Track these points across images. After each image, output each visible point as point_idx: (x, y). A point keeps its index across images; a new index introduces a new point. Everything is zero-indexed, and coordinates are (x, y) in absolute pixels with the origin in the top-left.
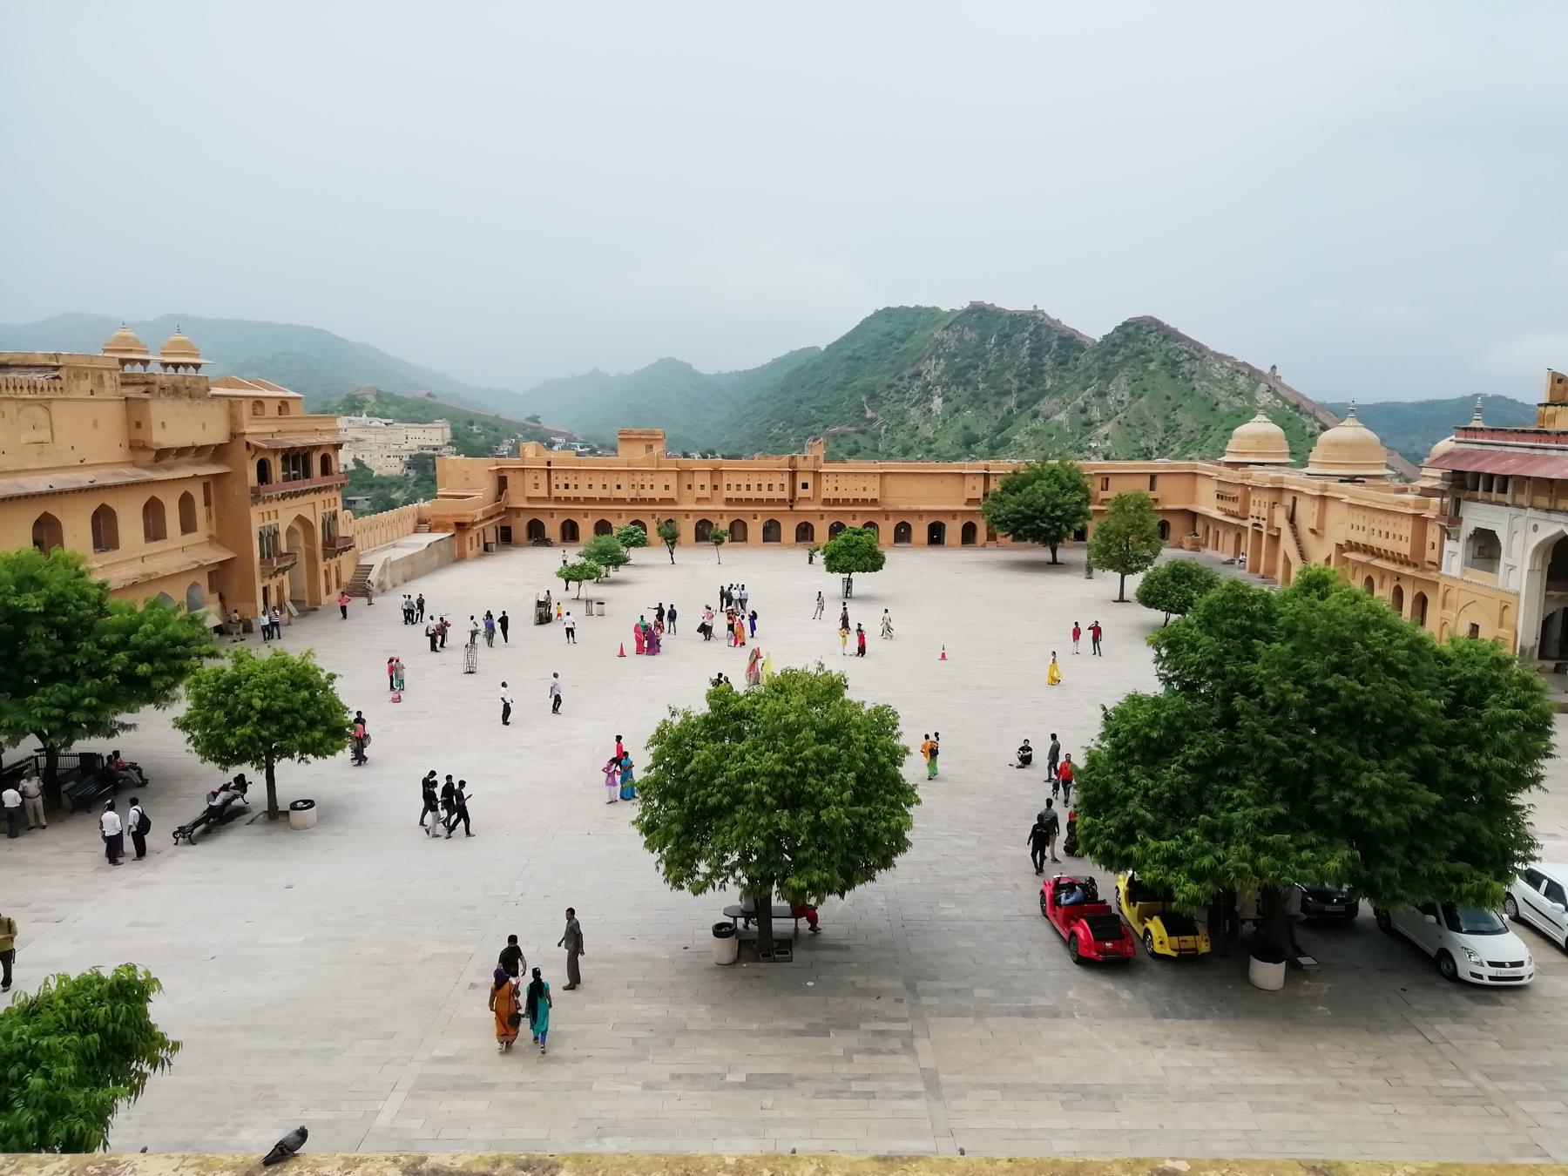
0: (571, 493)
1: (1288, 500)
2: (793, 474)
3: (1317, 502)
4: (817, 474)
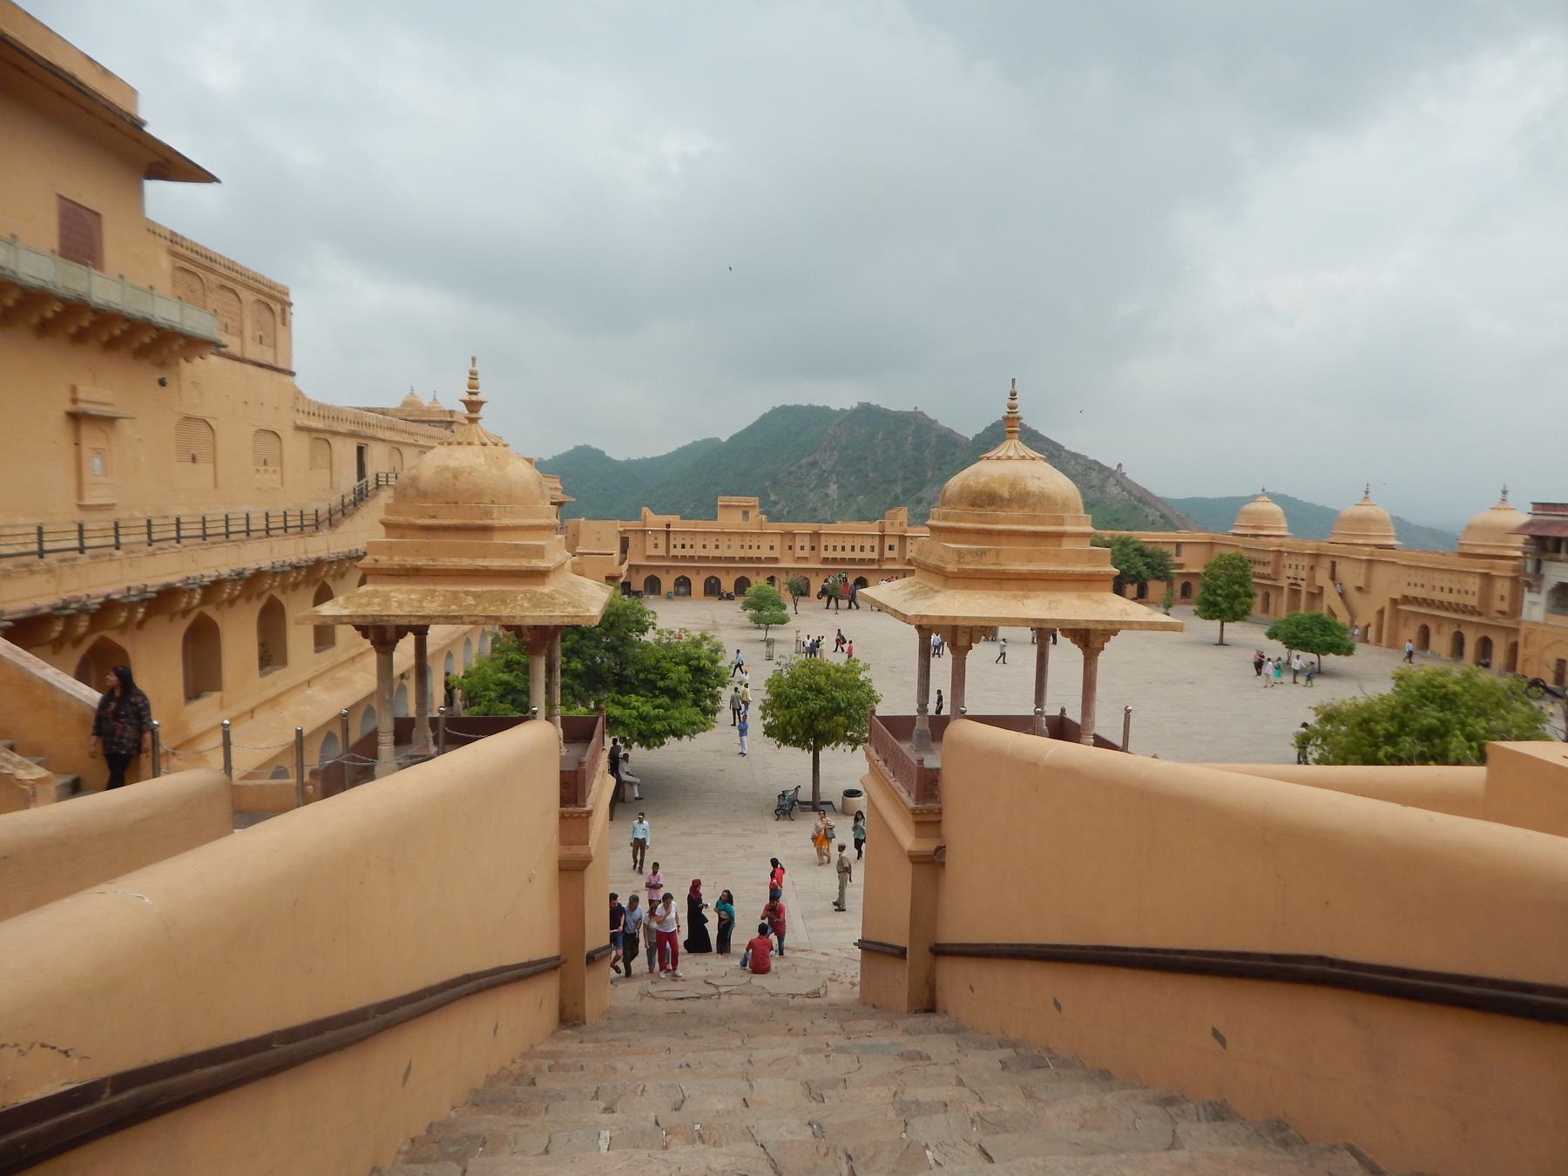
0: (688, 552)
1: (1327, 563)
2: (882, 537)
3: (1364, 566)
4: (903, 538)
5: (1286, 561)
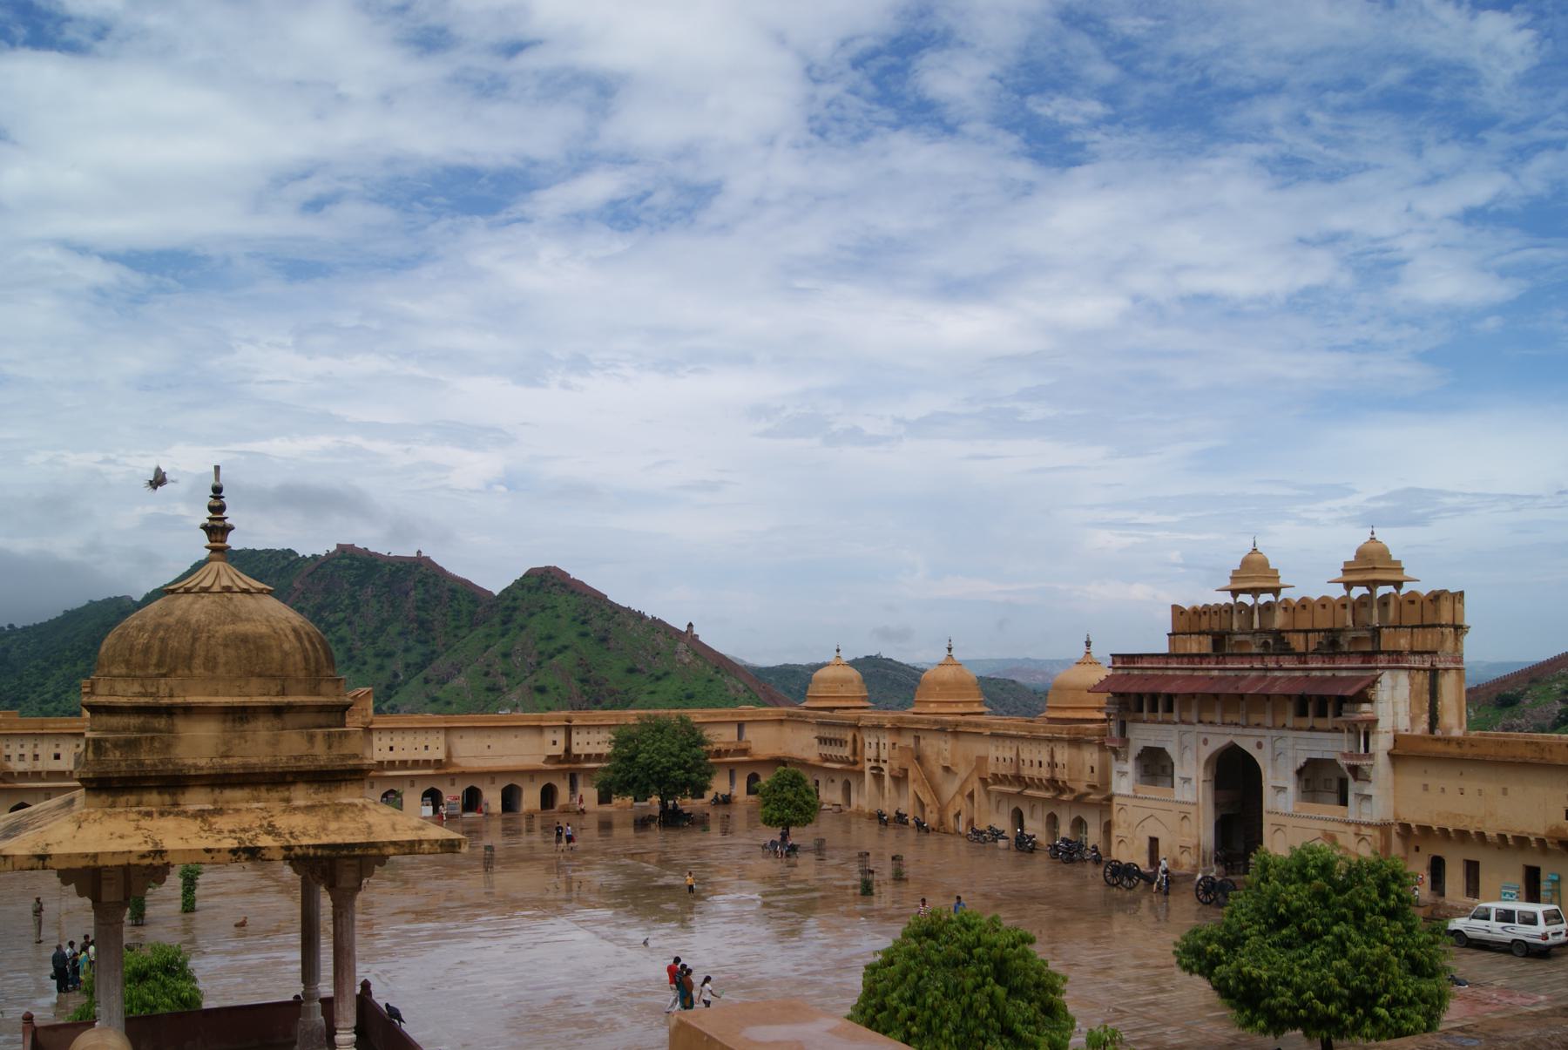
5: (869, 739)
